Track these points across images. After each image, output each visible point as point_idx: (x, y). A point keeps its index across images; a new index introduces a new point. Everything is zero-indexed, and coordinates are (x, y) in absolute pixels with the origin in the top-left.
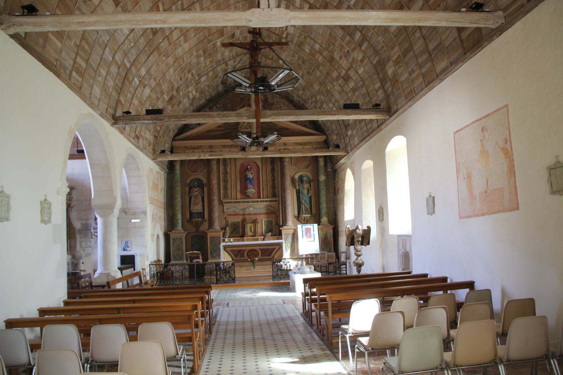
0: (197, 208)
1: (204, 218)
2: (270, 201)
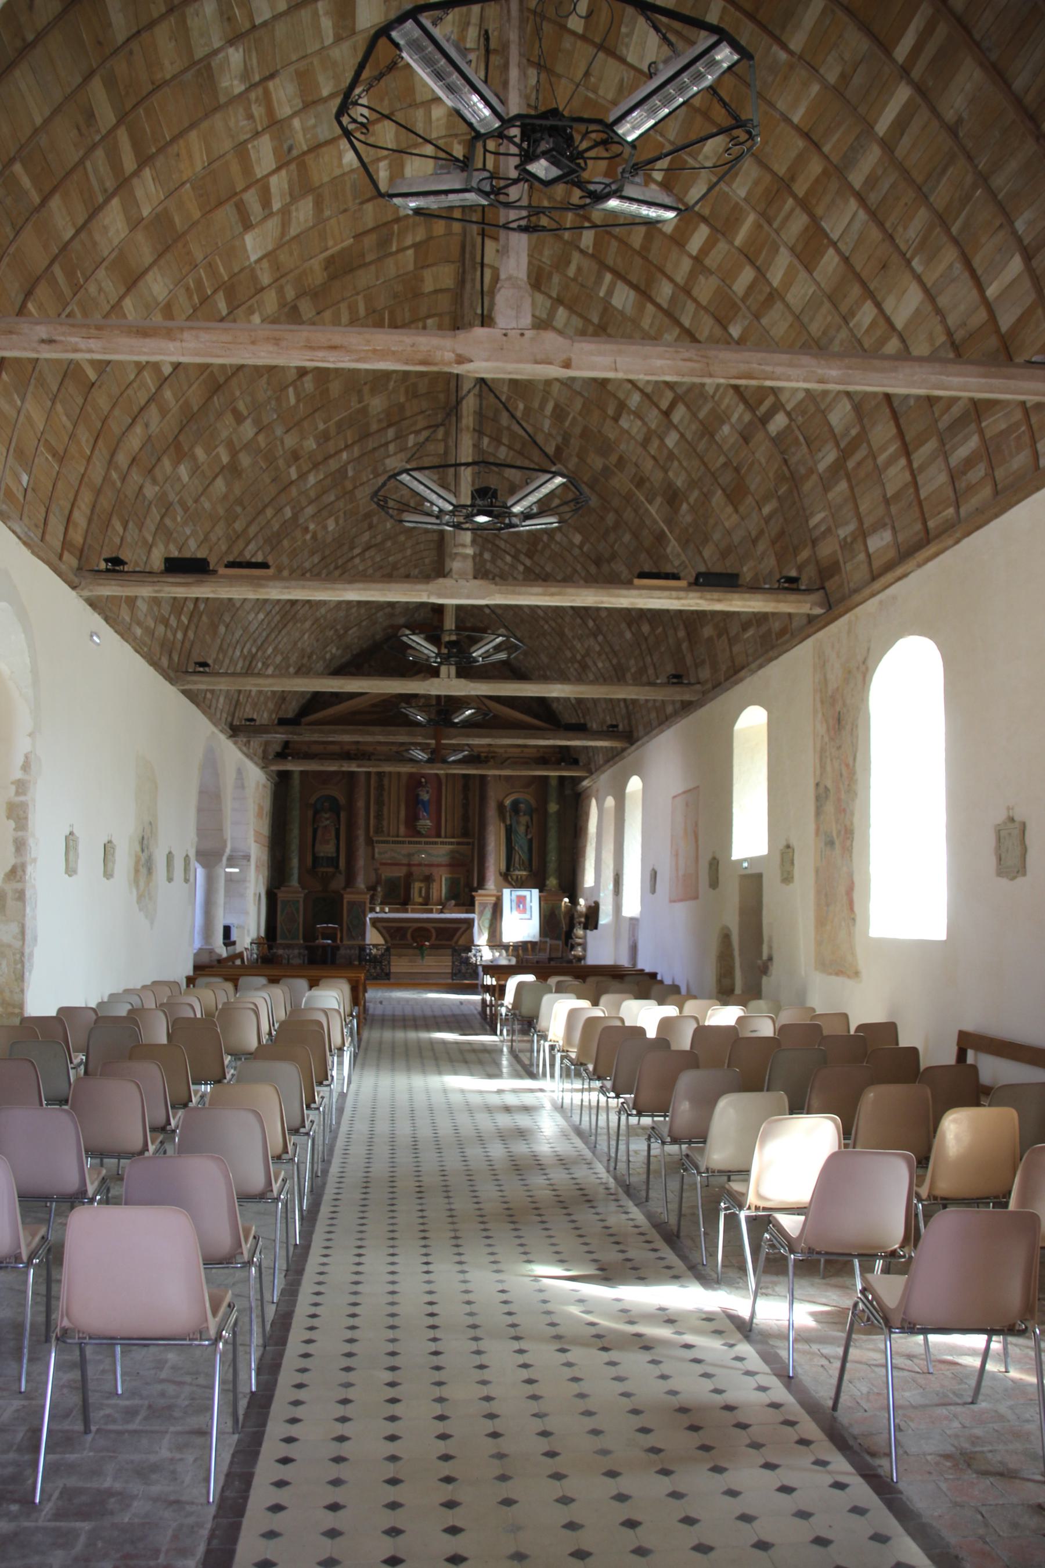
0: (327, 849)
1: (337, 867)
2: (458, 843)
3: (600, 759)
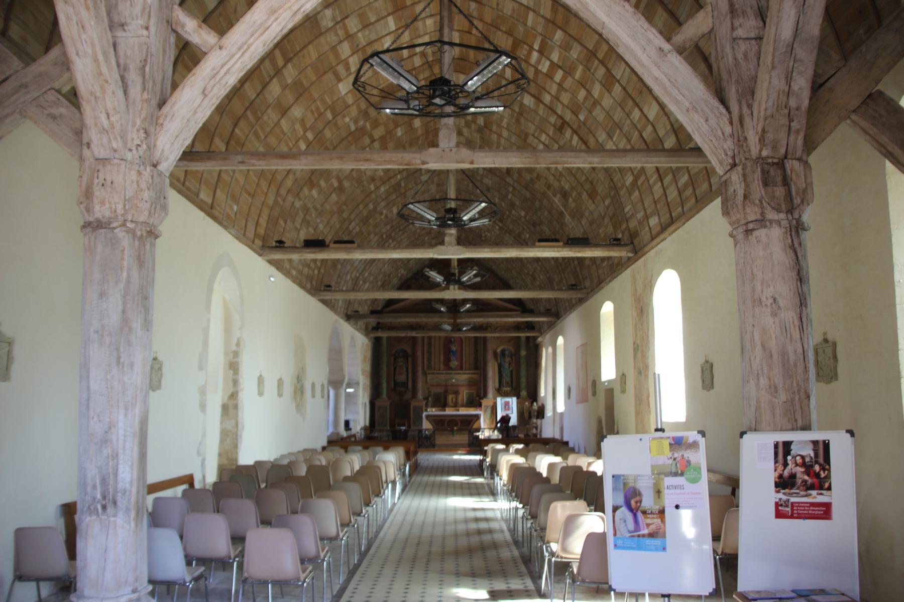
0: (402, 378)
3: (545, 326)
